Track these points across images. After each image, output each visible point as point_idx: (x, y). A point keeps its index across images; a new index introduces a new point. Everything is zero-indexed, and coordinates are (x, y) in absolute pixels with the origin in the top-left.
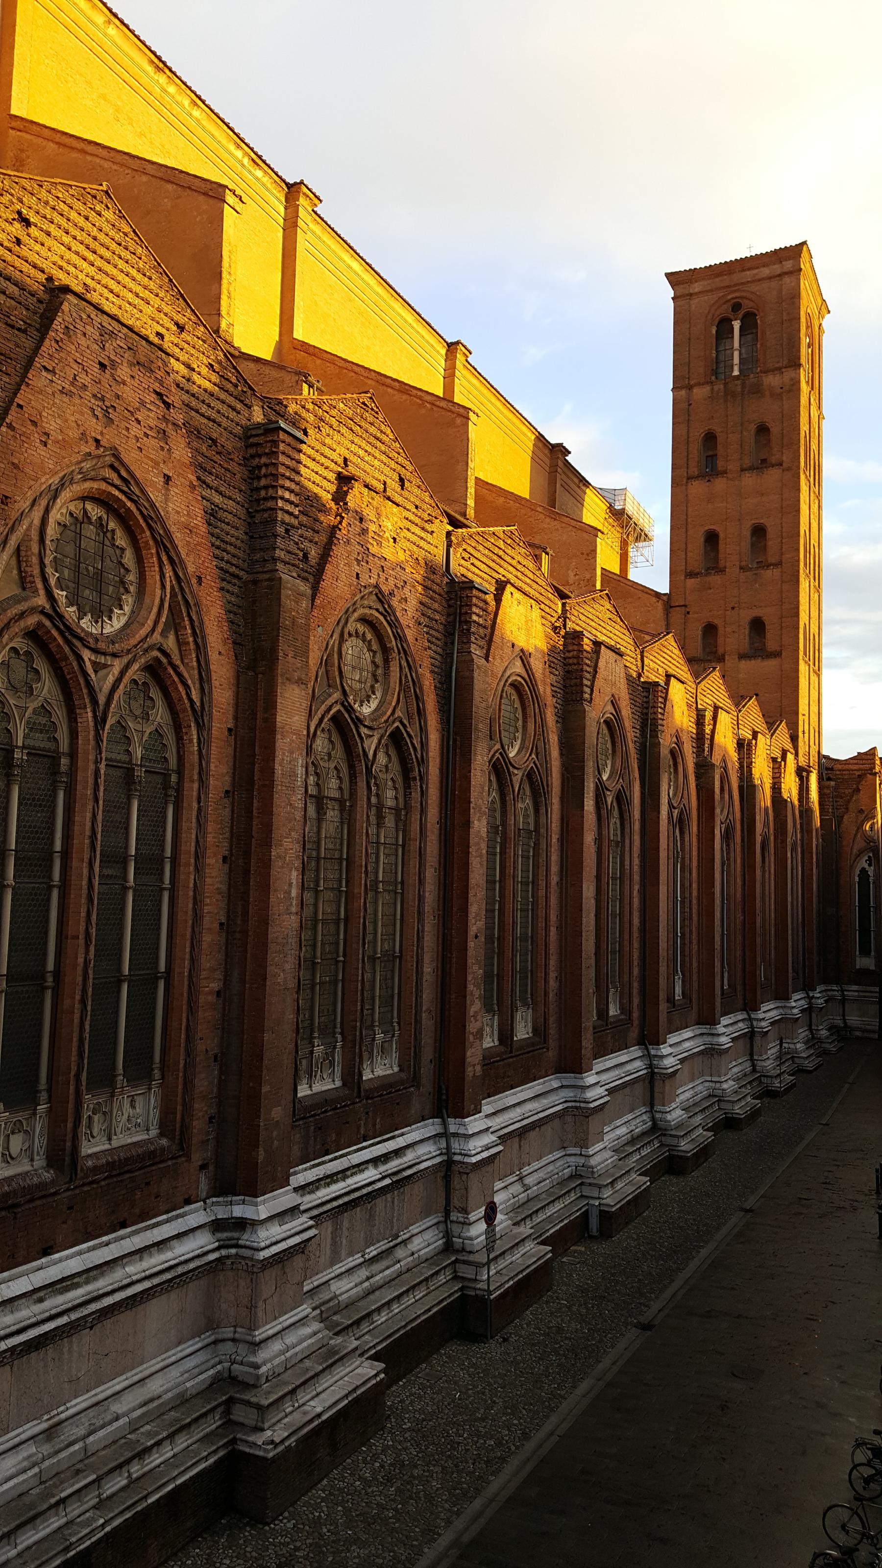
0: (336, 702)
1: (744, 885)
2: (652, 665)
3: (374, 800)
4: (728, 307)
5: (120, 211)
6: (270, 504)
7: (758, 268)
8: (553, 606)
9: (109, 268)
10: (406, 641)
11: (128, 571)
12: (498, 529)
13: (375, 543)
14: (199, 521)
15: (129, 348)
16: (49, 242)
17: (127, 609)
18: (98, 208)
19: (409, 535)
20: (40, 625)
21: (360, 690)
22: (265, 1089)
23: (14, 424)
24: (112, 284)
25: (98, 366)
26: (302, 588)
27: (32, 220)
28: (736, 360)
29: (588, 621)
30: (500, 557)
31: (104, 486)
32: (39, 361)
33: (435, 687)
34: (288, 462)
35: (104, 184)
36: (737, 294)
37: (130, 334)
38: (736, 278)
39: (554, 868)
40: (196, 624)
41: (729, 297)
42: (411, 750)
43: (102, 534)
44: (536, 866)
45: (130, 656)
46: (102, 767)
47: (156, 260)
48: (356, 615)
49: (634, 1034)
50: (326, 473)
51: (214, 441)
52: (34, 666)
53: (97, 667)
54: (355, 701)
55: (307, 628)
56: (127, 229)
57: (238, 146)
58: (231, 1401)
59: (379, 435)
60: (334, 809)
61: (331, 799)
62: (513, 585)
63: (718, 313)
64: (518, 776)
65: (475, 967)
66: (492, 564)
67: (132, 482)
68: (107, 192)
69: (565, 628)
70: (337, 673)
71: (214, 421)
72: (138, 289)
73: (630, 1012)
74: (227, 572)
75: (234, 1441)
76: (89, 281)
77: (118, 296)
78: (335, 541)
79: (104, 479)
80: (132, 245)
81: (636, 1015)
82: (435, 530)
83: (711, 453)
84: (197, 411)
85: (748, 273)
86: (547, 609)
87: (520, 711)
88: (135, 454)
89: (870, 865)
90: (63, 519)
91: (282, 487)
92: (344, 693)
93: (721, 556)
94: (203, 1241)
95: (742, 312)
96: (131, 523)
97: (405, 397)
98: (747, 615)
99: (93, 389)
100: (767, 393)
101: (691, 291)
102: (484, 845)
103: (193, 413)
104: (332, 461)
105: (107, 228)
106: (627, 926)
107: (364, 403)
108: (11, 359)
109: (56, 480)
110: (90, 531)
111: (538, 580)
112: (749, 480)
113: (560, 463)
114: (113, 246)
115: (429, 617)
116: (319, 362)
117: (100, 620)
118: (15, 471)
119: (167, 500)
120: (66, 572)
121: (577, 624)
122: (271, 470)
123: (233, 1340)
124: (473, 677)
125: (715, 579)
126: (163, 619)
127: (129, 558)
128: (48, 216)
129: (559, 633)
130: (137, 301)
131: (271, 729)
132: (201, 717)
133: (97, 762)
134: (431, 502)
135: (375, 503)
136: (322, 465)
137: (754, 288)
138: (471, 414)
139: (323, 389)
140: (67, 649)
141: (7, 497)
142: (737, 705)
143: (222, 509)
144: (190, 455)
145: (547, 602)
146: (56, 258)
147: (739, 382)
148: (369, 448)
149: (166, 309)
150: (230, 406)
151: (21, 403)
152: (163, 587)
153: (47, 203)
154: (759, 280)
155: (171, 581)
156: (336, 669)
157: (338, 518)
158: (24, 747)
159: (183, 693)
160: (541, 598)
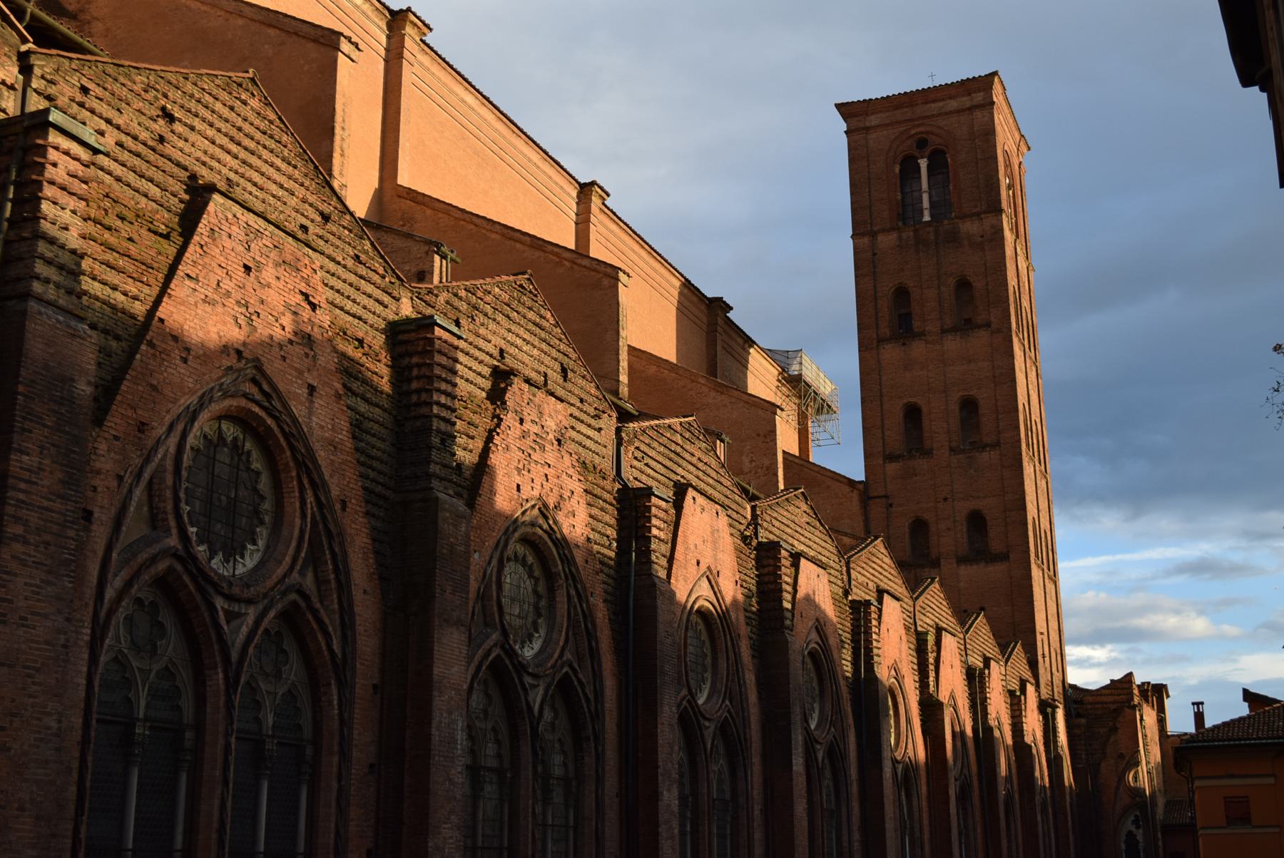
0: (495, 645)
2: (861, 579)
3: (540, 769)
5: (266, 98)
6: (424, 410)
7: (943, 100)
8: (741, 511)
9: (253, 160)
10: (575, 563)
11: (262, 498)
12: (674, 421)
13: (537, 448)
14: (344, 436)
15: (275, 246)
16: (193, 137)
17: (261, 543)
18: (243, 97)
19: (574, 434)
20: (170, 570)
21: (521, 627)
23: (154, 341)
24: (256, 177)
25: (243, 270)
26: (461, 509)
27: (176, 115)
28: (926, 204)
29: (783, 527)
30: (678, 454)
31: (243, 402)
32: (183, 269)
33: (609, 619)
34: (444, 360)
35: (251, 70)
37: (277, 231)
40: (339, 558)
41: (913, 132)
42: (583, 701)
43: (236, 459)
45: (266, 601)
46: (233, 740)
47: (301, 147)
48: (517, 535)
50: (480, 368)
51: (361, 342)
52: (160, 619)
53: (230, 616)
54: (515, 642)
55: (467, 555)
56: (272, 116)
59: (538, 320)
60: (491, 783)
61: (490, 769)
62: (695, 488)
64: (710, 729)
66: (669, 464)
67: (274, 396)
68: (252, 80)
69: (757, 538)
70: (495, 608)
71: (360, 318)
72: (282, 180)
74: (372, 492)
76: (232, 176)
77: (262, 189)
78: (493, 448)
79: (245, 396)
80: (276, 132)
82: (603, 426)
84: (342, 309)
85: (932, 105)
86: (735, 515)
87: (708, 643)
88: (278, 364)
89: (1138, 827)
90: (197, 442)
91: (439, 390)
92: (505, 633)
95: (928, 150)
96: (270, 442)
97: (538, 253)
99: (237, 295)
101: (868, 124)
102: (675, 823)
103: (338, 311)
104: (487, 353)
105: (252, 116)
107: (521, 286)
108: (153, 268)
109: (194, 399)
110: (224, 455)
111: (722, 480)
112: (952, 344)
114: (258, 135)
115: (599, 532)
116: (429, 212)
117: (232, 559)
118: (153, 394)
119: (311, 412)
120: (197, 503)
121: (770, 532)
122: (424, 371)
124: (655, 607)
125: (921, 464)
126: (303, 555)
127: (264, 484)
128: (193, 110)
129: (750, 544)
130: (280, 193)
131: (425, 684)
133: (227, 735)
134: (598, 393)
135: (536, 400)
136: (476, 359)
138: (621, 274)
139: (458, 260)
140: (198, 598)
141: (143, 424)
142: (962, 623)
143: (368, 418)
144: (336, 360)
145: (734, 506)
146: (199, 154)
147: (931, 229)
148: (527, 336)
149: (312, 199)
150: (377, 300)
151: (163, 316)
152: (304, 515)
153: (192, 96)
154: (946, 114)
155: (312, 508)
156: (495, 603)
157: (495, 420)
158: (146, 719)
159: (323, 644)
160: (727, 502)
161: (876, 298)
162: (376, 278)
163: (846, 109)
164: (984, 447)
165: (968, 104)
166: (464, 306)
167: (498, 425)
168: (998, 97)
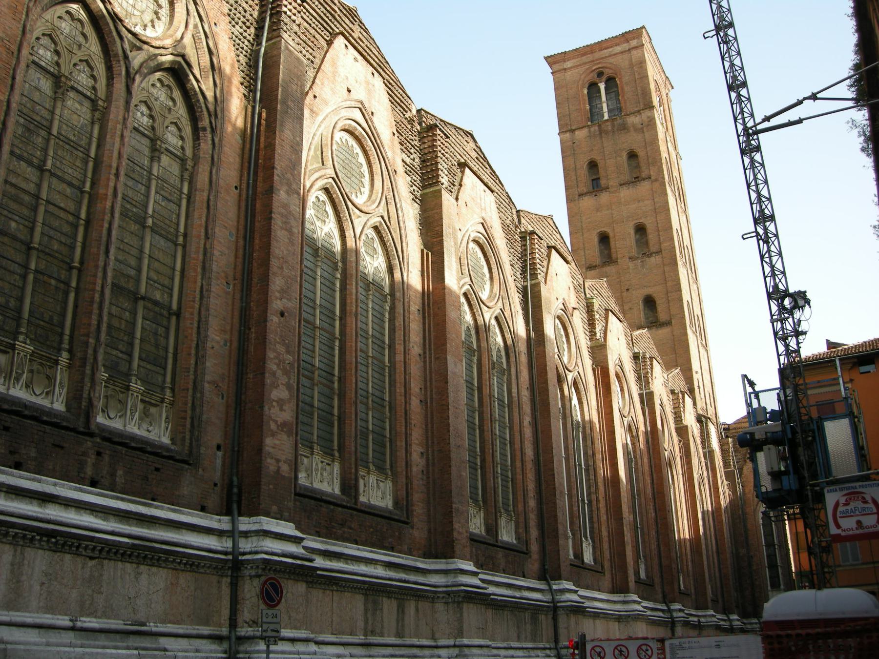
1: (653, 483)
4: (595, 75)
28: (605, 109)
36: (600, 66)
38: (597, 55)
41: (594, 68)
63: (587, 79)
65: (281, 349)
83: (594, 177)
93: (613, 250)
95: (604, 78)
100: (632, 129)
101: (565, 67)
106: (518, 453)
112: (625, 193)
137: (611, 60)
147: (609, 123)
154: (614, 55)
161: (575, 169)
163: (551, 60)
168: (645, 39)
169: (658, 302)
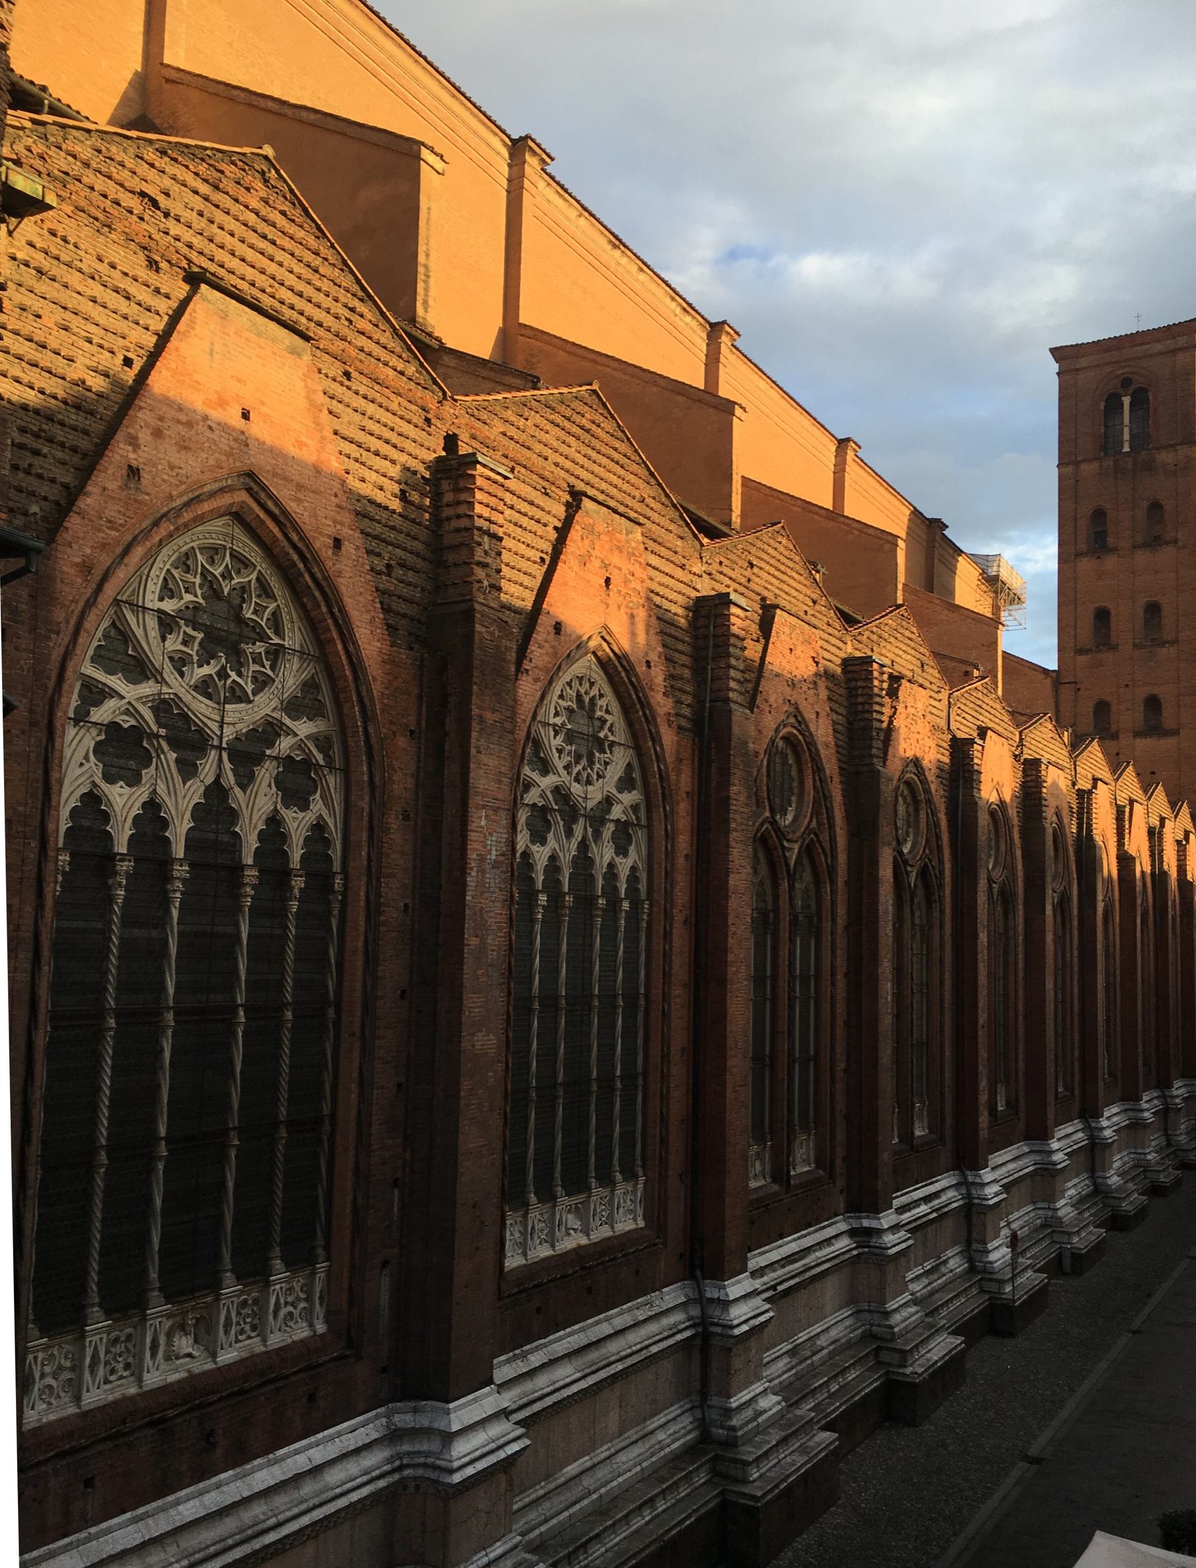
2: (1083, 772)
6: (867, 716)
22: (880, 1139)
28: (1126, 436)
36: (1127, 370)
39: (1021, 965)
44: (1006, 963)
49: (1076, 1108)
57: (673, 299)
58: (878, 1349)
66: (975, 714)
73: (1072, 1091)
75: (887, 1373)
76: (777, 591)
81: (1077, 1092)
94: (844, 1243)
95: (1133, 388)
98: (1142, 692)
112: (1142, 558)
113: (938, 538)
122: (866, 691)
123: (869, 1311)
125: (1107, 656)
132: (832, 870)
142: (1145, 791)
161: (1076, 519)
162: (836, 632)
164: (1163, 644)
165: (1172, 347)
166: (875, 638)
167: (895, 713)
169: (1164, 706)
